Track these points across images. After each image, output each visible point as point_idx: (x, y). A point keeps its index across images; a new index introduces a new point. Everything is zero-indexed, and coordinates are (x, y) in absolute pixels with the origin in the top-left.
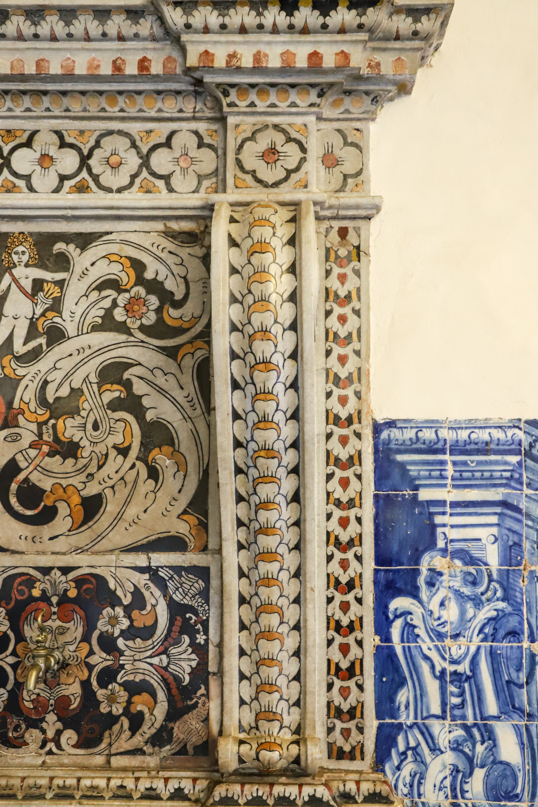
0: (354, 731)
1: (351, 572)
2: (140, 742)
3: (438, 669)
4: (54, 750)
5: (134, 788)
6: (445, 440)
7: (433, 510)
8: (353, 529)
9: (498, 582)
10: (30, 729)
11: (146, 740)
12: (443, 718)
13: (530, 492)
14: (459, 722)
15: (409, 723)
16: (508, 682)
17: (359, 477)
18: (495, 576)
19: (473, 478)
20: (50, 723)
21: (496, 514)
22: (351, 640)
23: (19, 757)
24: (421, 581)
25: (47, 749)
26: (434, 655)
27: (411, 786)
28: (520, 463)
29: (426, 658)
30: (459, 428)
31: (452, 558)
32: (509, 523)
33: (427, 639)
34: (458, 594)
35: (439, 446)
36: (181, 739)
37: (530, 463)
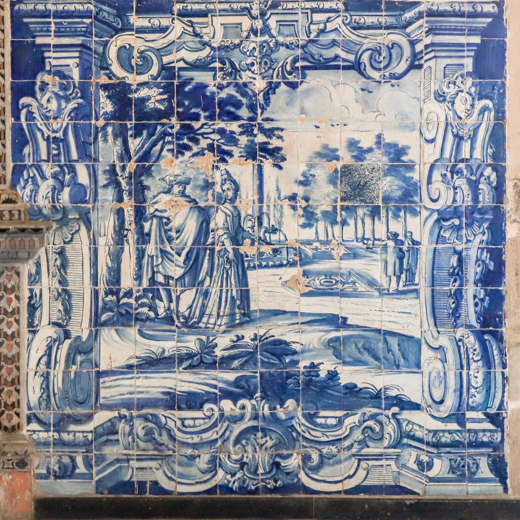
3: (46, 135)
6: (50, 11)
7: (43, 49)
9: (79, 88)
12: (48, 161)
13: (97, 39)
15: (30, 164)
18: (77, 85)
19: (65, 31)
21: (77, 51)
24: (37, 88)
26: (44, 128)
27: (31, 197)
28: (91, 23)
29: (40, 130)
30: (59, 4)
31: (54, 76)
33: (40, 120)
34: (56, 94)
35: (47, 13)
37: (97, 23)
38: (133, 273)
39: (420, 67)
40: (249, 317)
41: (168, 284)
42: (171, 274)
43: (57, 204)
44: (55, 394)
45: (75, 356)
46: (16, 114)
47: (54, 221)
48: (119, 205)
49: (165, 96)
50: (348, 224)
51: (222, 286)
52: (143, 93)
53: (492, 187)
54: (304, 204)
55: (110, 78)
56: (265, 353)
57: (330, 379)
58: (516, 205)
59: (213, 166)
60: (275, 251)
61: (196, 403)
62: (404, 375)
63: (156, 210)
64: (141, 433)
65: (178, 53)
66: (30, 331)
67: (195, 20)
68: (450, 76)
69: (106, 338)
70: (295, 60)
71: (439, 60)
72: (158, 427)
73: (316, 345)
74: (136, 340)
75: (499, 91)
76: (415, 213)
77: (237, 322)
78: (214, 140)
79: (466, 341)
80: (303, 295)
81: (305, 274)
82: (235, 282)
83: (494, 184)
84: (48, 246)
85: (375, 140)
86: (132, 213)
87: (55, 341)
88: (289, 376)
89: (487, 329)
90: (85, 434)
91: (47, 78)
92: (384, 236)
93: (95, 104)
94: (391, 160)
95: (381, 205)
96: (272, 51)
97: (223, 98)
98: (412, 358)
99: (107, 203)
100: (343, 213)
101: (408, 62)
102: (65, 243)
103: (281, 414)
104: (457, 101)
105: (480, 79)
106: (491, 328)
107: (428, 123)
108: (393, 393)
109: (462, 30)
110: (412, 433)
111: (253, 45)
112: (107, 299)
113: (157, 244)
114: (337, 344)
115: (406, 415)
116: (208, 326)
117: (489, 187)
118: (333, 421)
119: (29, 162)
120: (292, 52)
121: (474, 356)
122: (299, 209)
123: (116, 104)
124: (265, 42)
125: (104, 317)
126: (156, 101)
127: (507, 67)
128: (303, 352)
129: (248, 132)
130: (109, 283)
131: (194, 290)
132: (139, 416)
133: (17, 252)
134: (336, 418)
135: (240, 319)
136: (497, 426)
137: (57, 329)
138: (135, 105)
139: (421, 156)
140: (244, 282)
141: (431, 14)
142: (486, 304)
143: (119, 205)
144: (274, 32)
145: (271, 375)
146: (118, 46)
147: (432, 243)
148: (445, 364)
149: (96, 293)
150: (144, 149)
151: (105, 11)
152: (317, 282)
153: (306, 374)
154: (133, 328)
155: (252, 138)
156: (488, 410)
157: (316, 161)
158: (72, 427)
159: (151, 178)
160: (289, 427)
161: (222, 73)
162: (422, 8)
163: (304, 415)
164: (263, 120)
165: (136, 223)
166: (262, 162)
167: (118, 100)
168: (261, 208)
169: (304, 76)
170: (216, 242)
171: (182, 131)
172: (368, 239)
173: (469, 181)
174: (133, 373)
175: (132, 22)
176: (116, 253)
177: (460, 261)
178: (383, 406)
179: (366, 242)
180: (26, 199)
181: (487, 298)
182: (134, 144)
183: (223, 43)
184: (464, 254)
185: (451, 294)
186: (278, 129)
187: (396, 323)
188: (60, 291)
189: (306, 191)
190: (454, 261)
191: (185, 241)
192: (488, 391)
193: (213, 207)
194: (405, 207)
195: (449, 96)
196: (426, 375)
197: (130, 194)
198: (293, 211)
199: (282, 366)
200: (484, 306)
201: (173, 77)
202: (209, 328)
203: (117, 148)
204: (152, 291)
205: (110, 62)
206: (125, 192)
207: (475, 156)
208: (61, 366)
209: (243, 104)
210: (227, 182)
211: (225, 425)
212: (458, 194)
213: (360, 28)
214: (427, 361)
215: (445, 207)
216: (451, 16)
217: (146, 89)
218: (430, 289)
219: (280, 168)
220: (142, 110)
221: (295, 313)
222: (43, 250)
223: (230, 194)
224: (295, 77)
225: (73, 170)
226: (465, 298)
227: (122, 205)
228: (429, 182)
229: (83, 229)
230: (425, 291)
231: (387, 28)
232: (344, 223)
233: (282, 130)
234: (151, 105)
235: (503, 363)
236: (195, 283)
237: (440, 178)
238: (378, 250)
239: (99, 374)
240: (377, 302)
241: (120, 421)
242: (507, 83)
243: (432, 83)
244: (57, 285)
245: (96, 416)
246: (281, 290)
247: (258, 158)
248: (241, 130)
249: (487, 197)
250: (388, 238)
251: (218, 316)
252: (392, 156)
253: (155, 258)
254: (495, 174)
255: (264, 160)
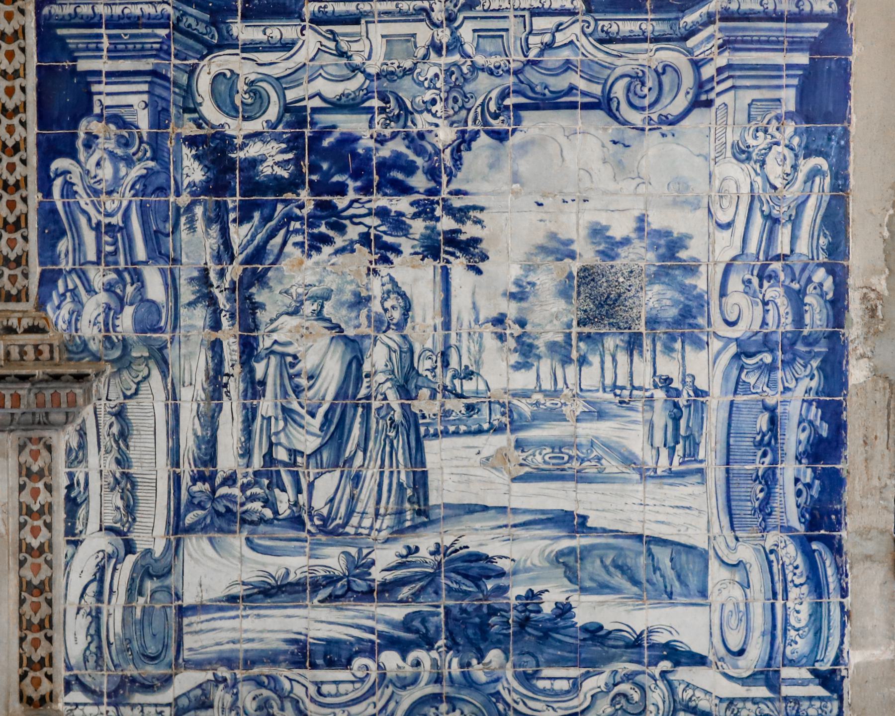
0: (20, 277)
1: (16, 137)
3: (94, 221)
6: (101, 15)
7: (90, 79)
8: (18, 97)
9: (148, 144)
12: (98, 263)
13: (178, 62)
14: (112, 267)
15: (68, 269)
16: (155, 232)
17: (23, 50)
18: (145, 138)
19: (126, 50)
21: (146, 82)
22: (17, 197)
26: (91, 210)
27: (70, 323)
28: (168, 36)
29: (84, 212)
30: (114, 4)
31: (107, 123)
32: (158, 91)
33: (85, 196)
34: (111, 154)
35: (96, 20)
37: (178, 35)
38: (237, 445)
39: (709, 104)
40: (427, 517)
41: (295, 464)
42: (300, 447)
43: (113, 335)
44: (109, 644)
45: (142, 581)
46: (45, 185)
47: (107, 361)
48: (214, 335)
49: (290, 156)
50: (590, 364)
51: (382, 465)
52: (254, 150)
53: (826, 301)
54: (517, 330)
55: (199, 126)
56: (453, 575)
57: (558, 616)
58: (866, 330)
59: (369, 269)
60: (470, 408)
61: (340, 656)
62: (680, 609)
63: (276, 342)
64: (251, 706)
65: (312, 83)
66: (68, 542)
67: (338, 29)
68: (759, 118)
69: (193, 553)
70: (504, 95)
71: (740, 93)
72: (279, 696)
73: (537, 562)
74: (242, 556)
75: (838, 143)
76: (699, 344)
77: (408, 524)
78: (370, 227)
79: (782, 553)
80: (514, 480)
81: (519, 445)
82: (405, 459)
83: (830, 296)
84: (98, 403)
85: (634, 225)
86: (236, 347)
87: (110, 557)
88: (493, 611)
89: (816, 533)
90: (159, 709)
91: (96, 127)
92: (648, 382)
93: (175, 169)
94: (662, 258)
95: (644, 332)
96: (465, 79)
97: (384, 158)
98: (693, 582)
99: (195, 332)
100: (582, 344)
101: (690, 96)
102: (126, 397)
103: (479, 673)
104: (770, 159)
105: (807, 123)
106: (822, 532)
107: (721, 197)
108: (661, 638)
109: (778, 42)
110: (693, 704)
111: (434, 70)
112: (195, 488)
113: (276, 398)
114: (571, 560)
115: (683, 674)
116: (360, 530)
117: (822, 302)
118: (564, 685)
119: (65, 265)
120: (498, 81)
121: (795, 578)
122: (509, 338)
123: (209, 169)
124: (455, 64)
125: (190, 519)
126: (276, 164)
127: (851, 103)
128: (515, 573)
129: (426, 213)
130: (198, 463)
131: (337, 473)
132: (247, 679)
133: (47, 414)
134: (569, 679)
135: (412, 519)
136: (831, 691)
137: (113, 537)
138: (241, 170)
139: (710, 251)
140: (419, 457)
141: (727, 16)
142: (815, 492)
143: (214, 335)
144: (469, 49)
145: (463, 610)
146: (213, 74)
147: (726, 394)
148: (748, 591)
149: (177, 480)
150: (256, 242)
151: (191, 15)
152: (539, 458)
153: (519, 608)
154: (237, 535)
155: (433, 223)
156: (817, 666)
157: (538, 259)
158: (138, 698)
159: (266, 290)
160: (492, 695)
161: (384, 116)
162: (712, 7)
163: (517, 676)
164: (450, 193)
165: (243, 364)
166: (448, 262)
167: (213, 162)
168: (447, 338)
169: (518, 121)
170: (374, 394)
171: (319, 213)
172: (623, 388)
173: (788, 291)
174: (238, 609)
175: (235, 34)
176: (210, 414)
177: (773, 421)
178: (646, 660)
179: (618, 392)
180: (62, 325)
181: (817, 482)
182: (239, 234)
183: (385, 67)
184: (779, 410)
185: (757, 476)
186: (475, 208)
187: (669, 524)
188: (118, 475)
189: (520, 310)
190: (763, 421)
191: (321, 394)
192: (818, 632)
193: (368, 336)
194: (683, 334)
195: (756, 151)
196: (716, 607)
197: (232, 316)
198: (499, 343)
199: (481, 596)
200: (812, 496)
201: (302, 123)
202: (361, 534)
203: (213, 241)
204: (269, 474)
205: (199, 100)
206: (224, 313)
207: (797, 251)
208: (120, 598)
209: (418, 168)
210: (392, 296)
211: (388, 692)
212: (771, 313)
213: (610, 40)
214: (718, 586)
215: (748, 334)
216: (760, 19)
217: (259, 144)
218: (723, 468)
219: (479, 272)
220: (251, 178)
221: (502, 509)
222: (90, 409)
223: (397, 315)
224: (503, 121)
225: (138, 278)
226: (781, 482)
227: (219, 335)
228: (723, 294)
229: (156, 374)
230: (715, 473)
231: (656, 40)
232: (583, 361)
233: (482, 209)
234: (266, 170)
235: (842, 589)
236: (339, 461)
237: (741, 287)
238: (639, 405)
239: (182, 611)
240: (637, 490)
241: (217, 686)
242: (853, 129)
243: (729, 130)
244: (114, 466)
245: (177, 680)
246: (480, 472)
247: (443, 255)
248: (414, 210)
249: (817, 317)
250: (656, 386)
251: (377, 514)
252: (662, 251)
253: (273, 420)
254: (831, 278)
255: (451, 259)
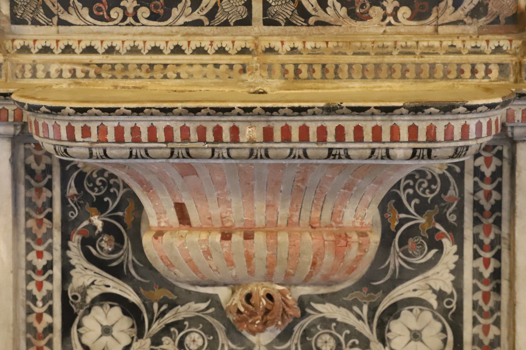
2: (461, 15)
4: (393, 22)
5: (462, 47)
10: (373, 7)
11: (466, 13)
20: (389, 2)
23: (365, 28)
25: (387, 21)
36: (495, 12)
